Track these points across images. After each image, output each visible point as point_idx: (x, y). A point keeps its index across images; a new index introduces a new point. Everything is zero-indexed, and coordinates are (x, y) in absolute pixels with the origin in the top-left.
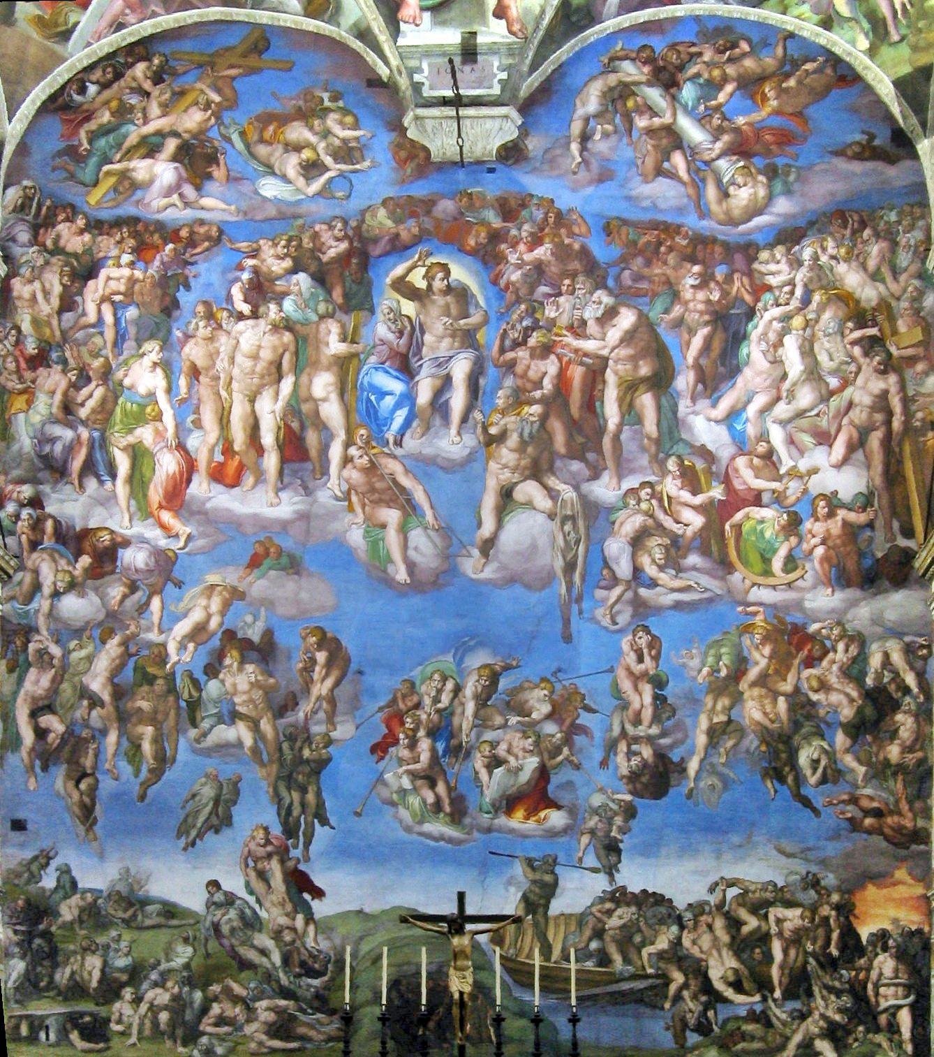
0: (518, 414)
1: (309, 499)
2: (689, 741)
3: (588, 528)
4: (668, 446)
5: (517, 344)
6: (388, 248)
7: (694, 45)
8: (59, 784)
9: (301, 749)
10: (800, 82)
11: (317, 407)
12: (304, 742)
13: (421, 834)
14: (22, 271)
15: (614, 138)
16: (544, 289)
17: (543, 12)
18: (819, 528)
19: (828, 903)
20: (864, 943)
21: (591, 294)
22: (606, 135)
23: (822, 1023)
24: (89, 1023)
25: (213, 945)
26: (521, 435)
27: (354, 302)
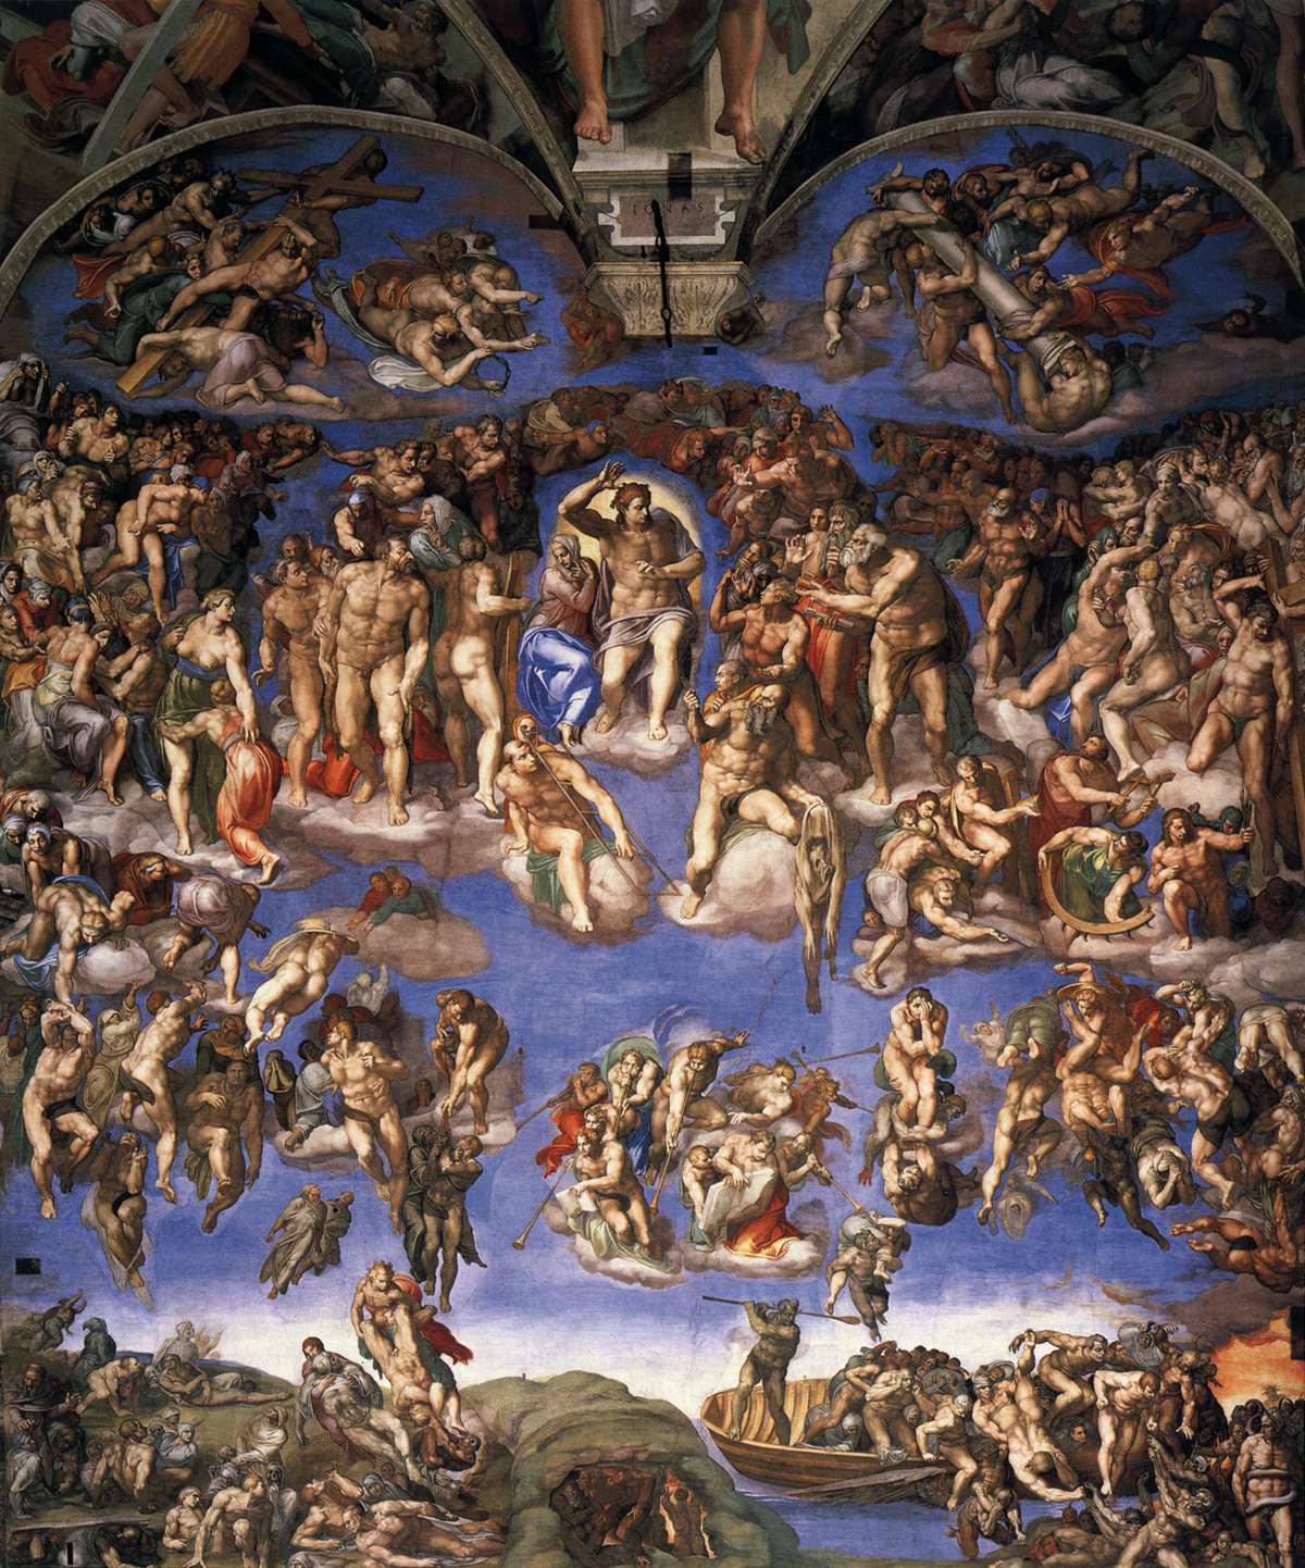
0: (747, 698)
1: (450, 816)
2: (986, 1147)
3: (844, 856)
4: (959, 742)
5: (744, 601)
6: (561, 462)
7: (1006, 169)
8: (88, 1209)
9: (438, 1157)
10: (1158, 224)
11: (460, 685)
12: (442, 1148)
13: (606, 1273)
14: (24, 485)
15: (888, 306)
16: (785, 522)
17: (790, 125)
18: (1171, 855)
19: (1177, 1365)
20: (1229, 1419)
21: (853, 529)
22: (876, 301)
23: (1168, 1528)
24: (130, 1538)
25: (312, 1427)
26: (751, 727)
27: (512, 538)
